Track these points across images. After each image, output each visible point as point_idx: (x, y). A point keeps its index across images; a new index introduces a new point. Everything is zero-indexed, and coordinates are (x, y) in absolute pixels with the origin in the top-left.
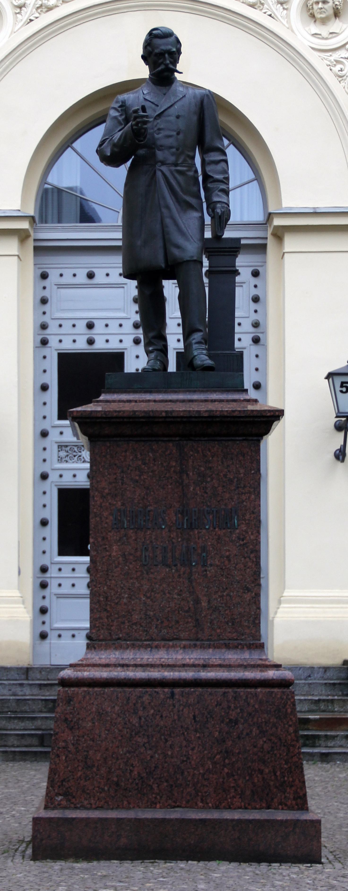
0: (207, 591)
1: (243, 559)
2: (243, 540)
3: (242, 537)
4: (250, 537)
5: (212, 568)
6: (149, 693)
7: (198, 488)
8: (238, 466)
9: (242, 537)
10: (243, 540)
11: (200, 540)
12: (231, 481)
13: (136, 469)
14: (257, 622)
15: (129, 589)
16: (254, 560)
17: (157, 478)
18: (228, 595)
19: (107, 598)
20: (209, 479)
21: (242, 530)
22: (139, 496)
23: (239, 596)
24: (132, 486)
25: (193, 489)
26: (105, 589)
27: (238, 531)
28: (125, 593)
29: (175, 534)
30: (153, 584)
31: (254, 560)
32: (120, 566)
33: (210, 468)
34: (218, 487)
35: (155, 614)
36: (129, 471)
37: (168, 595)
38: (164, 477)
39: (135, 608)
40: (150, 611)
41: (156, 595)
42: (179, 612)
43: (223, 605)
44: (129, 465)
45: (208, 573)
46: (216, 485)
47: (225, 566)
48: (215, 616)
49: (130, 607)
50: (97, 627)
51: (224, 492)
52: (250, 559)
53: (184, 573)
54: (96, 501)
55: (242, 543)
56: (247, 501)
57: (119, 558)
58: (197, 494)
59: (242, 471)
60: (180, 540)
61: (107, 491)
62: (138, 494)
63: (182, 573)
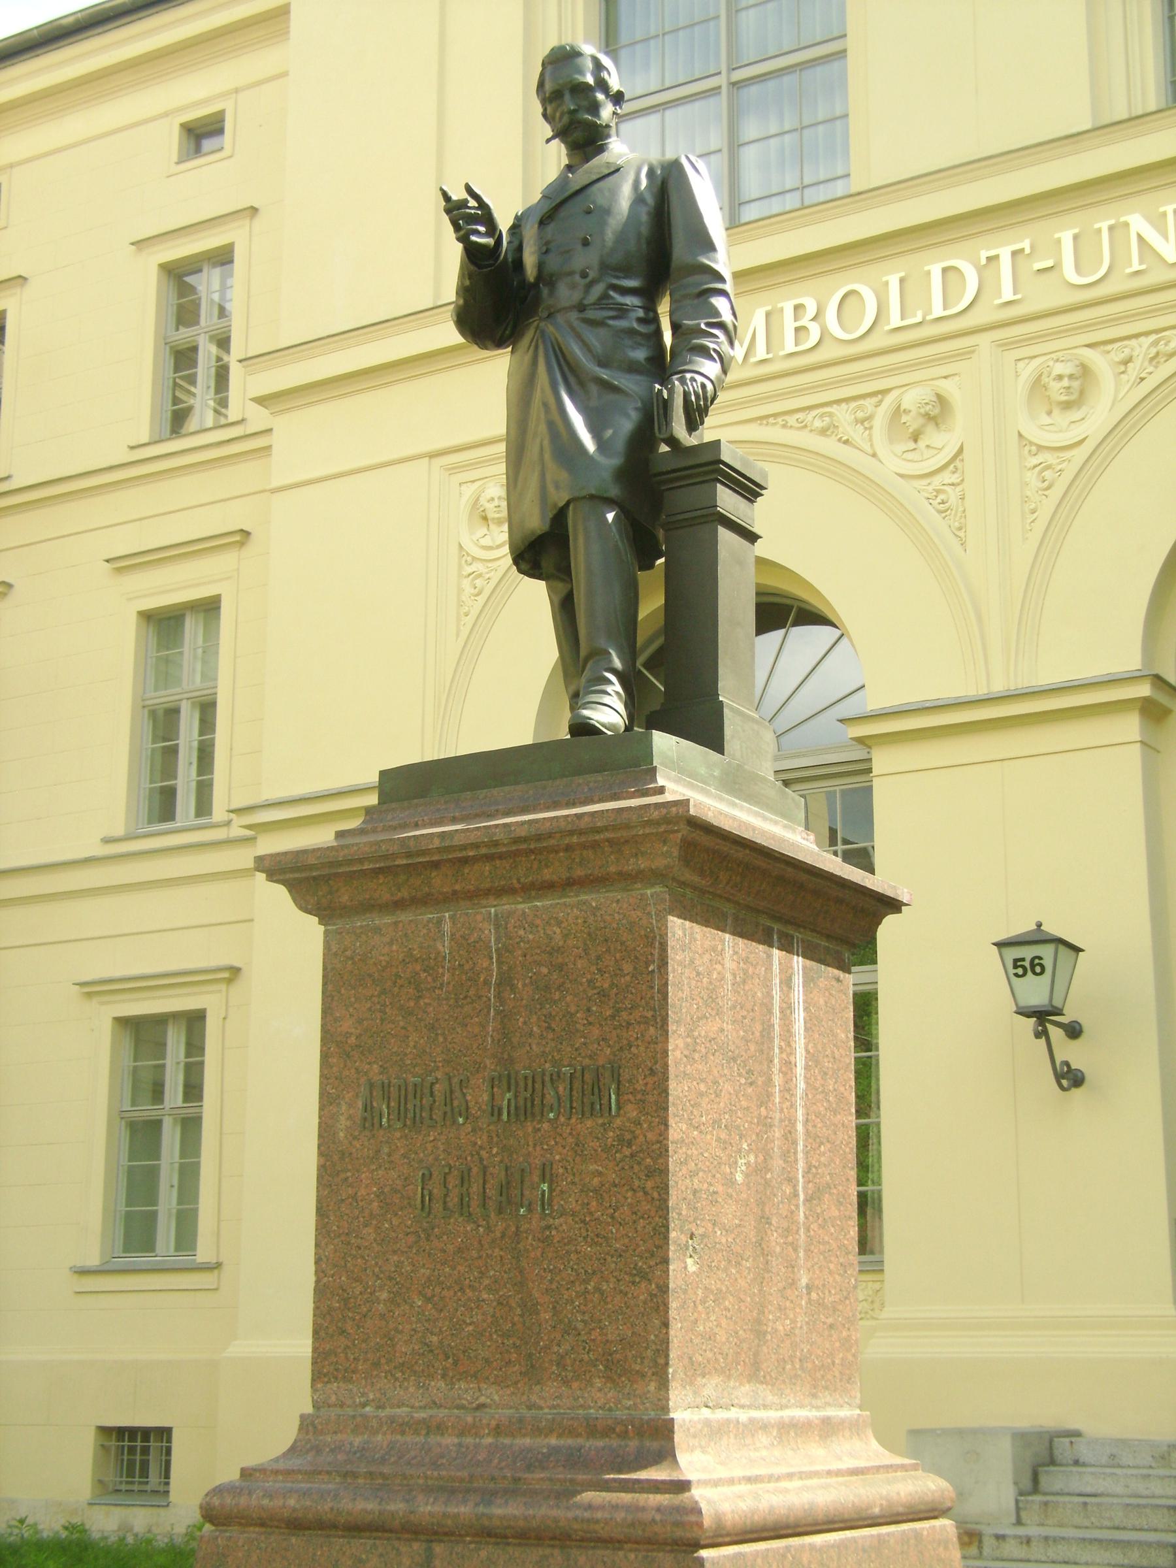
0: (551, 1281)
1: (630, 1194)
2: (630, 1145)
3: (628, 1136)
4: (645, 1136)
5: (562, 1220)
6: (380, 1550)
7: (534, 1019)
8: (618, 955)
9: (628, 1136)
10: (630, 1145)
11: (538, 1148)
12: (603, 994)
13: (410, 983)
14: (661, 1361)
15: (390, 1278)
16: (656, 1195)
17: (452, 1002)
18: (597, 1289)
19: (346, 1301)
20: (557, 996)
21: (629, 1119)
22: (415, 1047)
23: (621, 1292)
24: (402, 1024)
25: (525, 1023)
26: (343, 1278)
27: (618, 1122)
28: (381, 1288)
29: (485, 1137)
30: (438, 1266)
31: (656, 1195)
32: (374, 1222)
33: (561, 967)
34: (577, 1012)
35: (441, 1342)
36: (396, 990)
37: (469, 1293)
38: (466, 997)
39: (400, 1327)
40: (432, 1333)
41: (445, 1293)
42: (491, 1335)
43: (586, 1317)
44: (398, 976)
45: (554, 1232)
46: (573, 1009)
47: (591, 1213)
48: (568, 1347)
49: (391, 1325)
50: (325, 1375)
51: (590, 1024)
52: (646, 1193)
53: (503, 1236)
54: (332, 1067)
55: (627, 1152)
56: (639, 1042)
57: (372, 1201)
58: (531, 1034)
59: (627, 967)
60: (495, 1150)
61: (352, 1040)
62: (412, 1044)
63: (498, 1234)
